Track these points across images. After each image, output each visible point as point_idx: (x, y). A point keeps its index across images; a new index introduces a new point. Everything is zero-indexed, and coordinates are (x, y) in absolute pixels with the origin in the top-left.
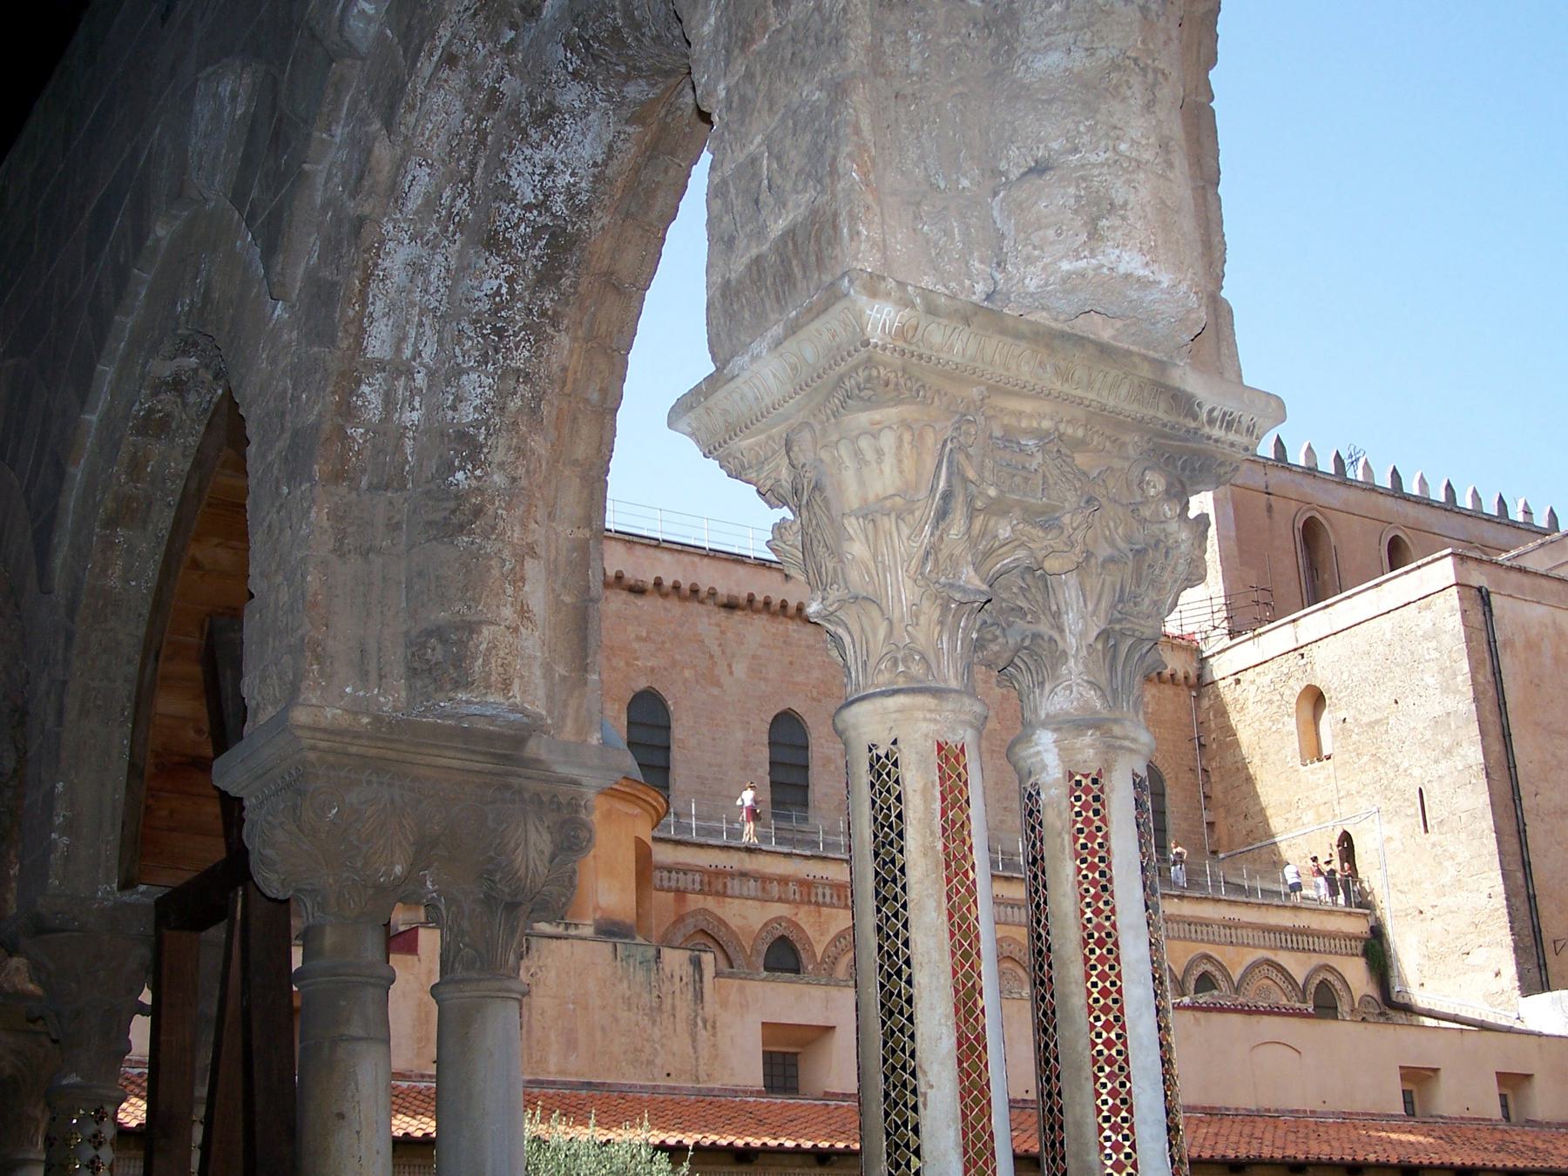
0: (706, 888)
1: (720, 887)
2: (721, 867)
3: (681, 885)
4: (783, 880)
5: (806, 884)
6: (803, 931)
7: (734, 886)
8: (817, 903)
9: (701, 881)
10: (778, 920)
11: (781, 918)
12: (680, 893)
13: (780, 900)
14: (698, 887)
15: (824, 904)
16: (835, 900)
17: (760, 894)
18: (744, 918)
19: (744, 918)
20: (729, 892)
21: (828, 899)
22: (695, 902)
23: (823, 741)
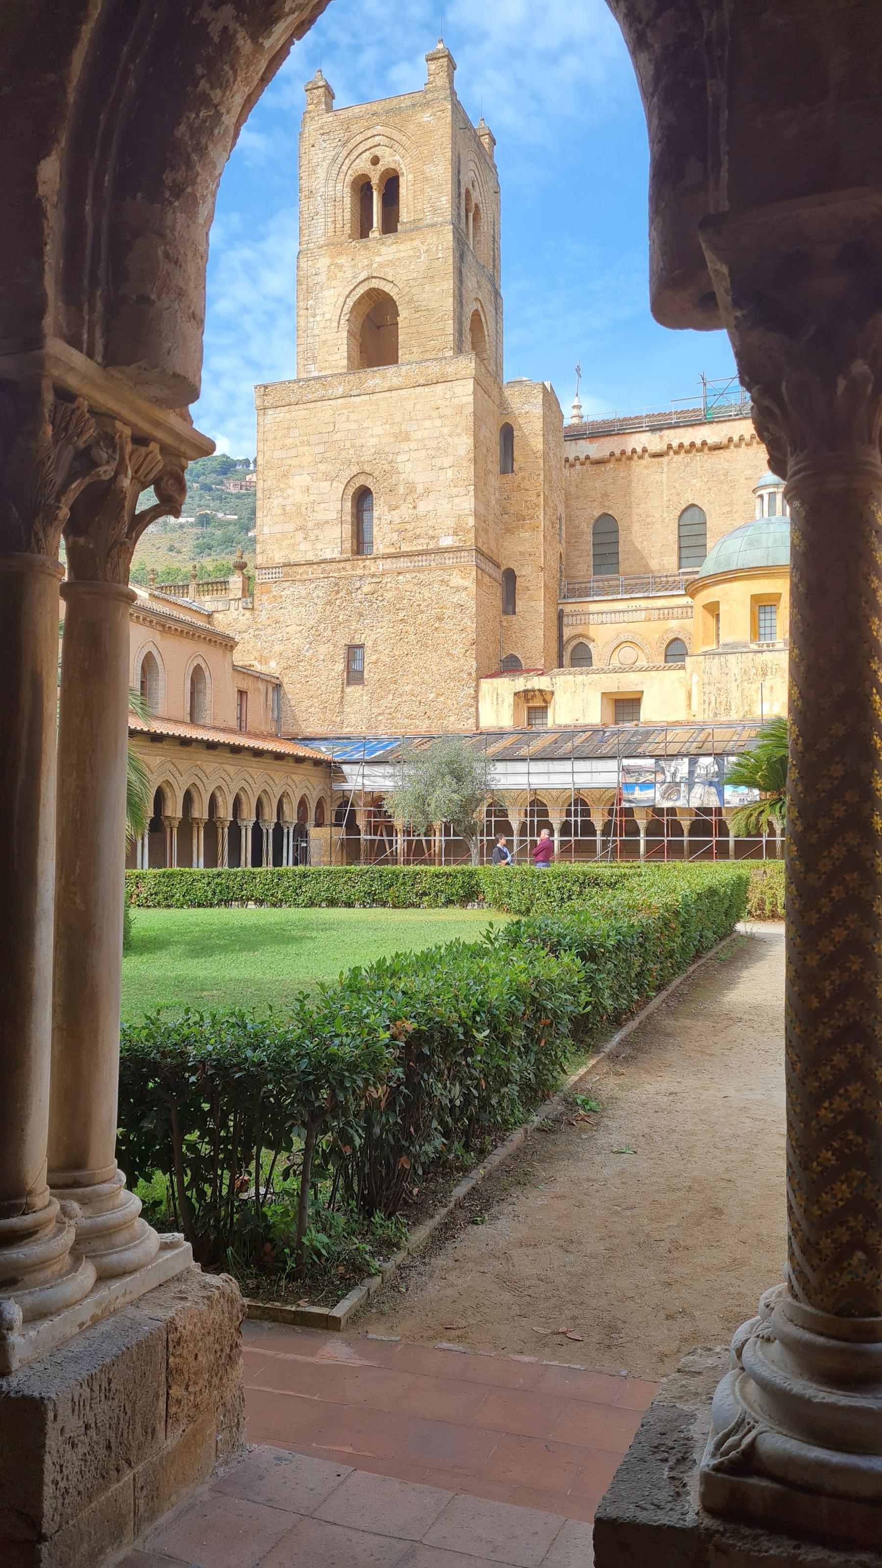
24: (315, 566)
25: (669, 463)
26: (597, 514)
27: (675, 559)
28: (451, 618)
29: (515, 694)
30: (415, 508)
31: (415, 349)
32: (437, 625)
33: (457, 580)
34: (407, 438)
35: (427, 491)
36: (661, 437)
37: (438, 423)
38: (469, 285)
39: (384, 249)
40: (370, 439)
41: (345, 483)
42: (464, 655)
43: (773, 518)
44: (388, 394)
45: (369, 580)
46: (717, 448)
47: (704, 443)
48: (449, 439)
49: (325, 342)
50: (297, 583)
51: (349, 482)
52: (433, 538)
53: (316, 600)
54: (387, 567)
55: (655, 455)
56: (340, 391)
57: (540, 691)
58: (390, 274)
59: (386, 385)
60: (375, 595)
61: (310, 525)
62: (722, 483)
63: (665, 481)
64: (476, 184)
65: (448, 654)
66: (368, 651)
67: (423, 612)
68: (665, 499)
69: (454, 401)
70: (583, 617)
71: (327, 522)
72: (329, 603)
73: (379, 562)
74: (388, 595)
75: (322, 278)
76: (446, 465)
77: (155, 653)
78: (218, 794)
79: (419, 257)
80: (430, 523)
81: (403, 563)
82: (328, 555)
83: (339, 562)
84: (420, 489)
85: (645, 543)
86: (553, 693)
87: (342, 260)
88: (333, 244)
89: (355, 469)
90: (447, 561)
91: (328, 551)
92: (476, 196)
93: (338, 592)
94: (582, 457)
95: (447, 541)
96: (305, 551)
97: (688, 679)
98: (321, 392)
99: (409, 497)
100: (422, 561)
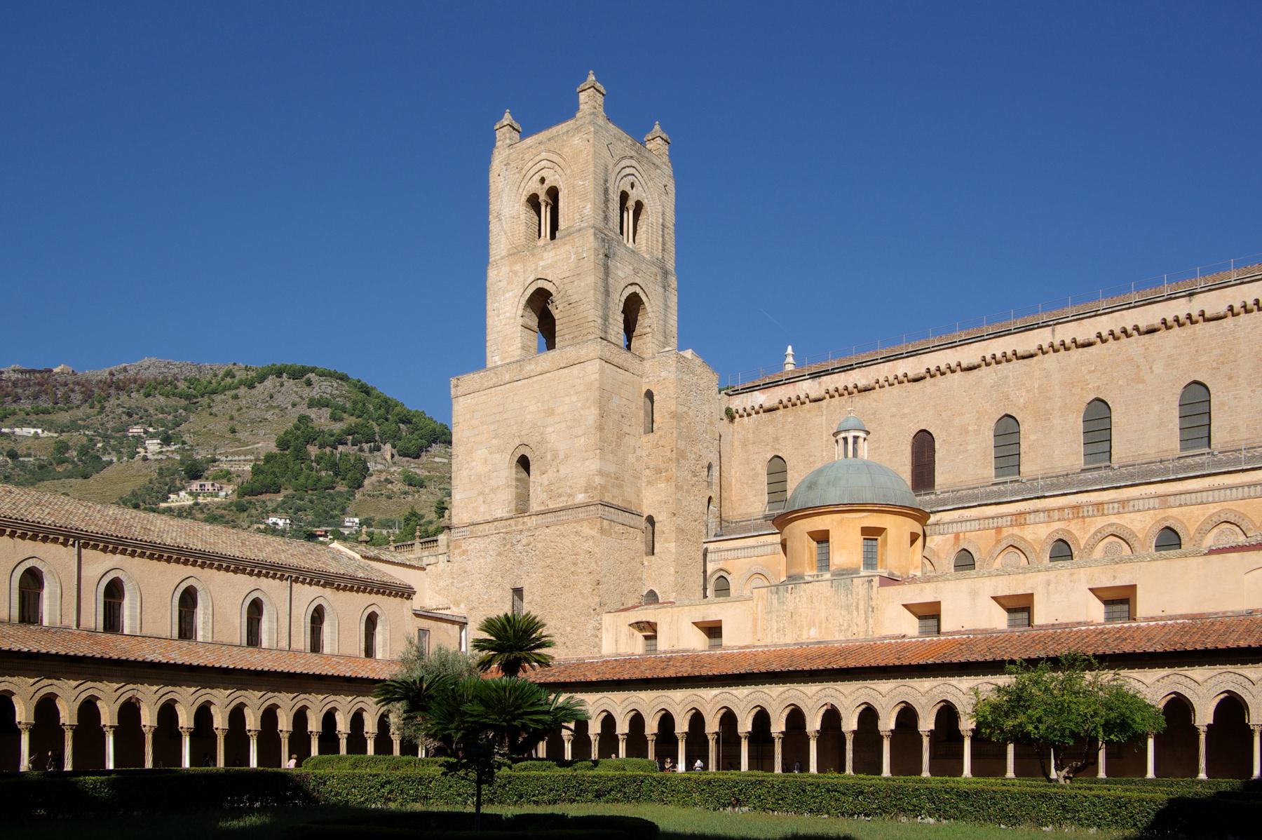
0: (1014, 523)
1: (1023, 521)
2: (1023, 510)
3: (1000, 525)
4: (1061, 509)
5: (1076, 508)
6: (1072, 534)
7: (1030, 518)
8: (1083, 517)
9: (1011, 520)
10: (1057, 531)
11: (1058, 530)
12: (999, 529)
13: (1059, 520)
14: (1009, 523)
15: (1089, 516)
16: (1095, 513)
17: (1046, 519)
18: (1036, 534)
19: (1036, 534)
20: (1028, 522)
21: (1090, 513)
22: (1006, 532)
23: (1220, 394)
24: (490, 524)
28: (583, 563)
29: (630, 625)
30: (558, 471)
31: (567, 337)
32: (573, 569)
33: (586, 530)
34: (551, 412)
35: (567, 457)
37: (574, 398)
38: (620, 273)
39: (546, 255)
40: (528, 416)
42: (592, 594)
44: (539, 377)
45: (526, 533)
48: (582, 411)
50: (479, 539)
52: (570, 495)
53: (492, 553)
54: (539, 522)
56: (507, 377)
57: (648, 622)
58: (550, 275)
59: (539, 370)
60: (531, 546)
61: (487, 490)
64: (637, 184)
65: (581, 594)
66: (525, 593)
67: (562, 558)
69: (586, 379)
70: (723, 553)
71: (498, 487)
72: (499, 554)
73: (534, 518)
74: (539, 545)
75: (503, 284)
76: (580, 433)
79: (570, 258)
80: (568, 484)
81: (550, 518)
82: (499, 516)
83: (506, 520)
84: (562, 456)
86: (656, 624)
87: (518, 267)
88: (511, 255)
89: (518, 442)
90: (580, 515)
91: (500, 511)
92: (634, 195)
93: (505, 546)
95: (580, 498)
96: (483, 513)
97: (755, 608)
98: (495, 380)
99: (554, 463)
100: (563, 516)
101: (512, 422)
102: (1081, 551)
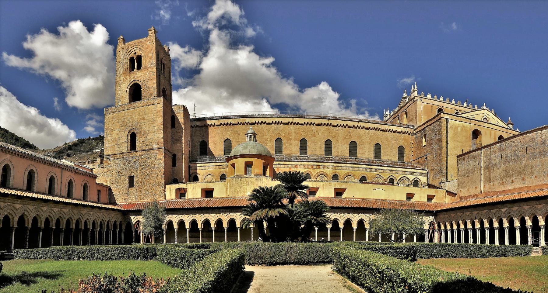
25: (221, 128)
26: (201, 140)
27: (223, 153)
36: (219, 121)
41: (128, 132)
43: (251, 142)
46: (233, 124)
47: (231, 123)
49: (123, 97)
51: (129, 131)
55: (217, 126)
62: (235, 133)
63: (220, 132)
68: (220, 137)
71: (123, 142)
77: (72, 179)
78: (87, 221)
85: (215, 148)
94: (196, 125)
101: (129, 122)
102: (313, 177)
